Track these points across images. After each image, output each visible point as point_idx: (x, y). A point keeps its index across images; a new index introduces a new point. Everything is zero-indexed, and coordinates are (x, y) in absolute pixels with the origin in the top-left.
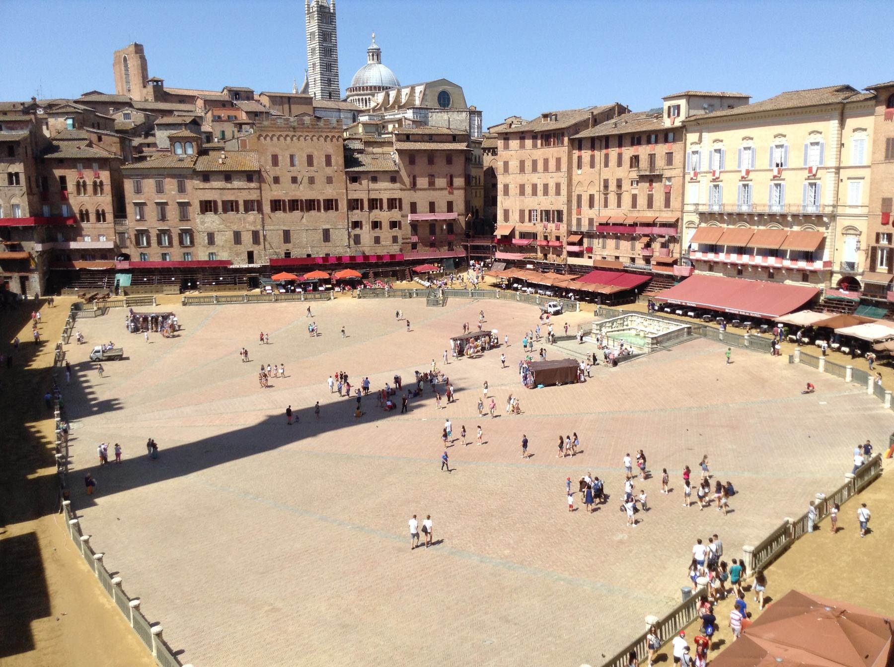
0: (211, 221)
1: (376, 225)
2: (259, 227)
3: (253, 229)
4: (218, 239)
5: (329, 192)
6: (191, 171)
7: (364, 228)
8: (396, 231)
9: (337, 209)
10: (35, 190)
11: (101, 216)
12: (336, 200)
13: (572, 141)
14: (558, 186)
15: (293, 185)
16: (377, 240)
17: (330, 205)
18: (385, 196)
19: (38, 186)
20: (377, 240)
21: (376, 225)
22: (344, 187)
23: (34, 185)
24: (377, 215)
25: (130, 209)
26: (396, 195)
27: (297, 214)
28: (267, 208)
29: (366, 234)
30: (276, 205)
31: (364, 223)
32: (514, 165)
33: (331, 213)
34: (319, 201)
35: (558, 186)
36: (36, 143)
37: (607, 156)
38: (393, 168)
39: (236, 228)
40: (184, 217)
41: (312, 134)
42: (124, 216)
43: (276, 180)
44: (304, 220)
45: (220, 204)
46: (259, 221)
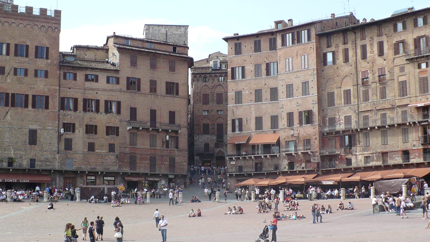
1: (91, 129)
5: (41, 87)
7: (77, 131)
8: (112, 139)
9: (47, 107)
12: (47, 98)
13: (320, 36)
14: (305, 84)
16: (91, 147)
17: (40, 102)
18: (102, 98)
20: (91, 147)
21: (91, 129)
22: (57, 84)
24: (90, 118)
26: (115, 97)
29: (79, 138)
31: (77, 125)
32: (250, 68)
34: (27, 96)
35: (305, 84)
37: (364, 48)
38: (112, 68)
41: (27, 22)
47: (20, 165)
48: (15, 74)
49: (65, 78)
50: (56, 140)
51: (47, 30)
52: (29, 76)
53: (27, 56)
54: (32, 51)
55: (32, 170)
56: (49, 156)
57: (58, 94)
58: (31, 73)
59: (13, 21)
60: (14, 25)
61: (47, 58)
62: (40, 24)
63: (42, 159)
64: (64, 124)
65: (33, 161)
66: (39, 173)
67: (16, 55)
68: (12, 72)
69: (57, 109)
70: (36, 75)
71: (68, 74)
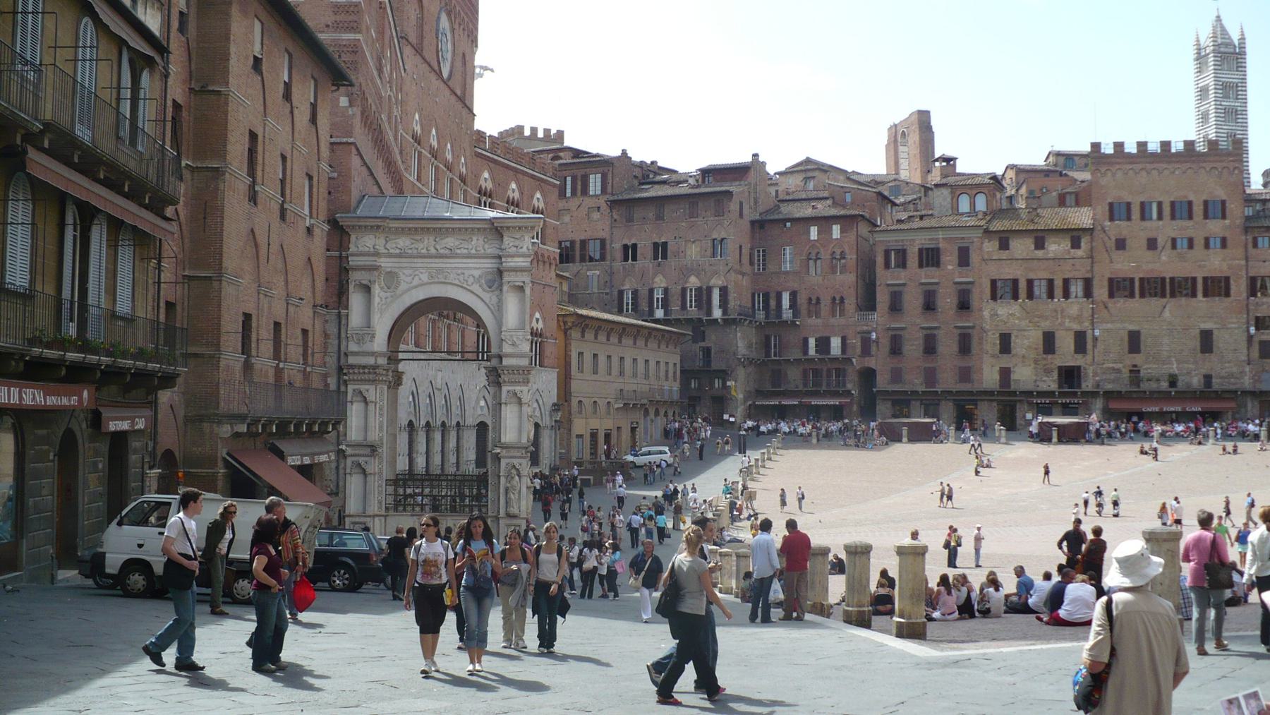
0: (1007, 313)
2: (1087, 324)
3: (1077, 327)
4: (1019, 345)
5: (1216, 263)
6: (979, 233)
9: (1227, 294)
10: (747, 268)
11: (838, 303)
12: (1227, 279)
15: (1150, 253)
17: (1217, 287)
19: (752, 263)
23: (746, 259)
25: (882, 298)
27: (1155, 303)
28: (1100, 291)
30: (1119, 287)
33: (1219, 304)
34: (1194, 280)
36: (756, 202)
39: (1046, 325)
40: (964, 305)
42: (872, 308)
43: (1121, 244)
44: (1167, 314)
45: (1023, 286)
46: (1087, 313)
47: (1189, 385)
48: (1174, 246)
49: (1255, 245)
50: (1244, 344)
51: (1221, 173)
52: (1196, 247)
53: (1190, 217)
54: (1198, 210)
55: (1207, 391)
56: (1235, 370)
57: (1244, 273)
58: (1199, 242)
59: (1165, 166)
60: (1166, 172)
61: (1224, 217)
62: (1208, 166)
63: (1223, 373)
64: (1257, 319)
65: (1208, 379)
66: (1219, 396)
67: (1173, 217)
68: (1169, 244)
69: (1245, 295)
70: (1207, 246)
71: (1260, 239)
